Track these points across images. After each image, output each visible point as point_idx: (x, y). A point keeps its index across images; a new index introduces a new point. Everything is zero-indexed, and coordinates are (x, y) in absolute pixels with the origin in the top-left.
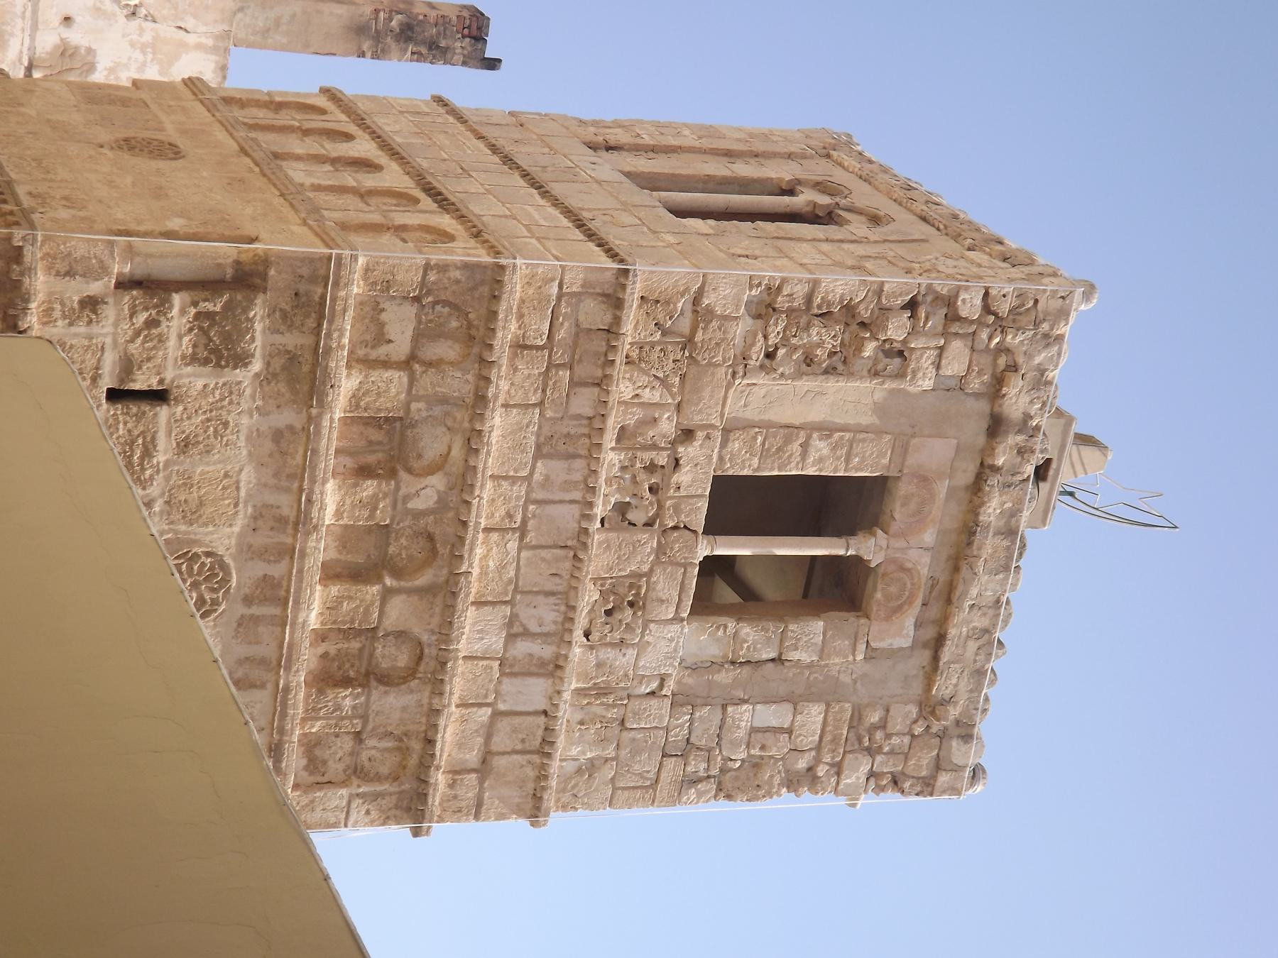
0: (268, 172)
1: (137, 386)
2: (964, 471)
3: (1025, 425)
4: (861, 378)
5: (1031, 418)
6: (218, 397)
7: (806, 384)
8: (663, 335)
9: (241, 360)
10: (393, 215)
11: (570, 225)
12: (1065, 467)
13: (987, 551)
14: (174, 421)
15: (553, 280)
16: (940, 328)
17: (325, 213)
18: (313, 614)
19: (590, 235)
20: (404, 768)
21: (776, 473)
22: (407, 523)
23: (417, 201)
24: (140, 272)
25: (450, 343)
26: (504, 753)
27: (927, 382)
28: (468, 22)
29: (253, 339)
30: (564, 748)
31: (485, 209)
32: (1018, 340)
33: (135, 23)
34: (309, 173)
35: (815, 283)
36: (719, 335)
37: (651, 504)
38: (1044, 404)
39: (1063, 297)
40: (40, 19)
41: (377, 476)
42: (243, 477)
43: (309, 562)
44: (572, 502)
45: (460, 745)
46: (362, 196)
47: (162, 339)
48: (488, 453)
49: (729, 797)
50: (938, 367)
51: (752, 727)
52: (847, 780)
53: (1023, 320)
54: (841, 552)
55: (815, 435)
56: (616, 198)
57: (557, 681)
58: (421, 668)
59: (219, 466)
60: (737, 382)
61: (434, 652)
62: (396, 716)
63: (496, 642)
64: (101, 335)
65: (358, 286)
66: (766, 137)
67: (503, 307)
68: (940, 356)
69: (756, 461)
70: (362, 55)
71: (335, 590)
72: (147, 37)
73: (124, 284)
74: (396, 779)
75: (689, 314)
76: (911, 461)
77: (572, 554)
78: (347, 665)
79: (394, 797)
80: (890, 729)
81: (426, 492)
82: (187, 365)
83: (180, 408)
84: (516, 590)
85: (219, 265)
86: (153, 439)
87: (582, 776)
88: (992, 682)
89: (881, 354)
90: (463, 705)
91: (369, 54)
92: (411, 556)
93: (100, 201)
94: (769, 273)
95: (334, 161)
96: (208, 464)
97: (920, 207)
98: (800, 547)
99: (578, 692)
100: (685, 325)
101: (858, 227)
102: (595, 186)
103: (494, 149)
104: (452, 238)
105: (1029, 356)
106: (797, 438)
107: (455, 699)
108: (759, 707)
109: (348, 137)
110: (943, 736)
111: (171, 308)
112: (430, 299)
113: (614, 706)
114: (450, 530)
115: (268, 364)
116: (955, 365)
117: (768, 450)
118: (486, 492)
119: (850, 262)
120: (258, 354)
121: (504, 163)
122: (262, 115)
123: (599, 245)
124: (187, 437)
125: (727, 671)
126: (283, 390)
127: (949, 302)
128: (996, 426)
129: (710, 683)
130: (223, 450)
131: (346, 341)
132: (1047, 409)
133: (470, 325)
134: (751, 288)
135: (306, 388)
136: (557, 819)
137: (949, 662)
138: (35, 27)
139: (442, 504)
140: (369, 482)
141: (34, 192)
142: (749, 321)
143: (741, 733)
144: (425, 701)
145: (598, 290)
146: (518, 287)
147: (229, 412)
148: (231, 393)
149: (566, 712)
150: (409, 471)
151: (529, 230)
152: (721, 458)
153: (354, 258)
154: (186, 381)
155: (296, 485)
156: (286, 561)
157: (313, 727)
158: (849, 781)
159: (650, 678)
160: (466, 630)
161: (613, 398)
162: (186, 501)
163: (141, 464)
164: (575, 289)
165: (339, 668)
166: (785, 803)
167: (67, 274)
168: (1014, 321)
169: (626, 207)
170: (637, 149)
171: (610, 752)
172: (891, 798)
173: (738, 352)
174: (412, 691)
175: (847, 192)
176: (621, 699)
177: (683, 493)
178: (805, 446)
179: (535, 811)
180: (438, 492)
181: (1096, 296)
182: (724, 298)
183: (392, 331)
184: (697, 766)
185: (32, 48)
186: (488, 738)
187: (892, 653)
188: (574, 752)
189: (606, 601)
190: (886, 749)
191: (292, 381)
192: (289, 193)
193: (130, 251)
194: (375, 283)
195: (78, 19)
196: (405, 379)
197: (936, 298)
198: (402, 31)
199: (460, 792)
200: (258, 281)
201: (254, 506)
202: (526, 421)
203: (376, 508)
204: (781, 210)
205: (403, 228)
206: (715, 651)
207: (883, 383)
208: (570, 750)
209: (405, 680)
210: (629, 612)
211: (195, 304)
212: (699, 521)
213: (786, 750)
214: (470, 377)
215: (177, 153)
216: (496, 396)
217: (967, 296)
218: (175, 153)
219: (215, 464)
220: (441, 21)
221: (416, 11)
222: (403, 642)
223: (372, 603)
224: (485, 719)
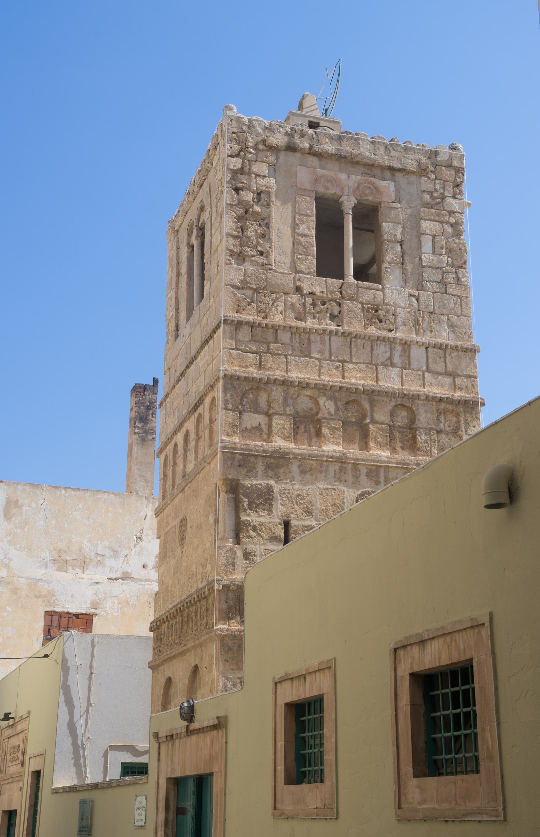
0: (190, 480)
2: (312, 161)
3: (290, 135)
4: (270, 211)
5: (287, 132)
6: (286, 499)
7: (274, 237)
8: (253, 302)
9: (270, 489)
10: (205, 425)
12: (312, 114)
13: (349, 149)
14: (297, 518)
15: (230, 353)
16: (247, 176)
17: (205, 454)
18: (383, 454)
19: (211, 337)
20: (453, 411)
21: (315, 248)
22: (341, 414)
23: (200, 414)
24: (232, 534)
25: (260, 397)
26: (446, 366)
27: (272, 181)
28: (138, 393)
29: (260, 484)
30: (443, 339)
32: (251, 140)
33: (143, 537)
34: (191, 462)
35: (228, 235)
36: (252, 277)
37: (330, 304)
38: (280, 126)
39: (231, 120)
40: (145, 578)
41: (320, 427)
42: (322, 487)
43: (360, 456)
44: (330, 340)
45: (442, 386)
46: (199, 438)
47: (261, 524)
48: (308, 378)
49: (465, 263)
50: (265, 176)
51: (432, 254)
52: (457, 208)
53: (242, 138)
54: (351, 216)
55: (297, 231)
56: (196, 325)
57: (412, 343)
58: (407, 405)
59: (317, 497)
60: (274, 268)
61: (399, 399)
62: (429, 415)
63: (394, 372)
64: (260, 550)
65: (235, 439)
66: (171, 259)
67: (243, 375)
68: (259, 176)
69: (310, 258)
71: (372, 445)
73: (238, 541)
74: (458, 414)
75: (244, 291)
76: (308, 187)
77: (353, 339)
78: (406, 438)
79: (467, 415)
81: (327, 406)
82: (272, 513)
83: (292, 515)
84: (371, 364)
85: (228, 500)
86: (306, 526)
87: (456, 330)
88: (410, 143)
89: (259, 203)
90: (424, 385)
91: (154, 436)
92: (356, 411)
94: (223, 255)
95: (186, 450)
96: (316, 502)
97: (196, 188)
98: (348, 235)
99: (417, 333)
100: (249, 293)
101: (205, 216)
102: (192, 335)
103: (178, 381)
104: (214, 398)
105: (258, 135)
106: (299, 239)
107: (421, 389)
108: (423, 251)
109: (176, 445)
110: (435, 165)
111: (247, 520)
112: (240, 407)
113: (423, 317)
114: (344, 394)
115: (271, 477)
117: (304, 252)
118: (326, 379)
119: (219, 219)
121: (184, 376)
122: (169, 483)
123: (215, 333)
124: (305, 512)
125: (406, 266)
126: (282, 470)
127: (235, 173)
128: (291, 148)
129: (412, 274)
130: (310, 496)
131: (260, 443)
132: (283, 125)
133: (251, 389)
134: (231, 264)
135: (281, 460)
136: (475, 342)
137: (401, 164)
138: (148, 580)
139: (332, 398)
140: (323, 431)
141: (201, 580)
142: (246, 264)
143: (435, 258)
144: (422, 402)
145: (234, 332)
146: (234, 368)
147: (293, 494)
148: (284, 493)
149: (427, 339)
150: (317, 413)
151: (210, 364)
152: (309, 273)
153: (222, 441)
154: (279, 513)
155: (325, 463)
156: (358, 466)
157: (435, 452)
158: (457, 208)
159: (410, 301)
160: (389, 385)
161: (282, 323)
162: (333, 512)
164: (234, 343)
165: (408, 441)
166: (468, 237)
168: (242, 143)
169: (200, 321)
170: (177, 317)
171: (444, 318)
172: (465, 187)
173: (260, 268)
174: (418, 409)
175: (191, 222)
176: (420, 314)
177: (325, 290)
178: (302, 235)
179: (472, 351)
180: (327, 400)
181: (230, 105)
182: (236, 275)
183: (255, 423)
184: (450, 279)
186: (439, 373)
187: (397, 191)
188: (445, 334)
189: (375, 323)
190: (442, 191)
191: (278, 467)
192: (198, 470)
193: (223, 539)
194: (234, 432)
195: (144, 562)
196: (276, 417)
197: (233, 179)
198: (143, 422)
199: (464, 385)
200: (234, 483)
201: (335, 481)
202: (294, 362)
203: (335, 428)
204: (200, 251)
206: (397, 272)
207: (273, 201)
208: (444, 336)
209: (413, 412)
211: (245, 510)
212: (337, 282)
213: (443, 237)
214: (274, 388)
216: (283, 376)
217: (232, 165)
218: (184, 520)
219: (316, 500)
220: (138, 405)
221: (134, 416)
222: (396, 413)
223: (378, 428)
224: (430, 375)
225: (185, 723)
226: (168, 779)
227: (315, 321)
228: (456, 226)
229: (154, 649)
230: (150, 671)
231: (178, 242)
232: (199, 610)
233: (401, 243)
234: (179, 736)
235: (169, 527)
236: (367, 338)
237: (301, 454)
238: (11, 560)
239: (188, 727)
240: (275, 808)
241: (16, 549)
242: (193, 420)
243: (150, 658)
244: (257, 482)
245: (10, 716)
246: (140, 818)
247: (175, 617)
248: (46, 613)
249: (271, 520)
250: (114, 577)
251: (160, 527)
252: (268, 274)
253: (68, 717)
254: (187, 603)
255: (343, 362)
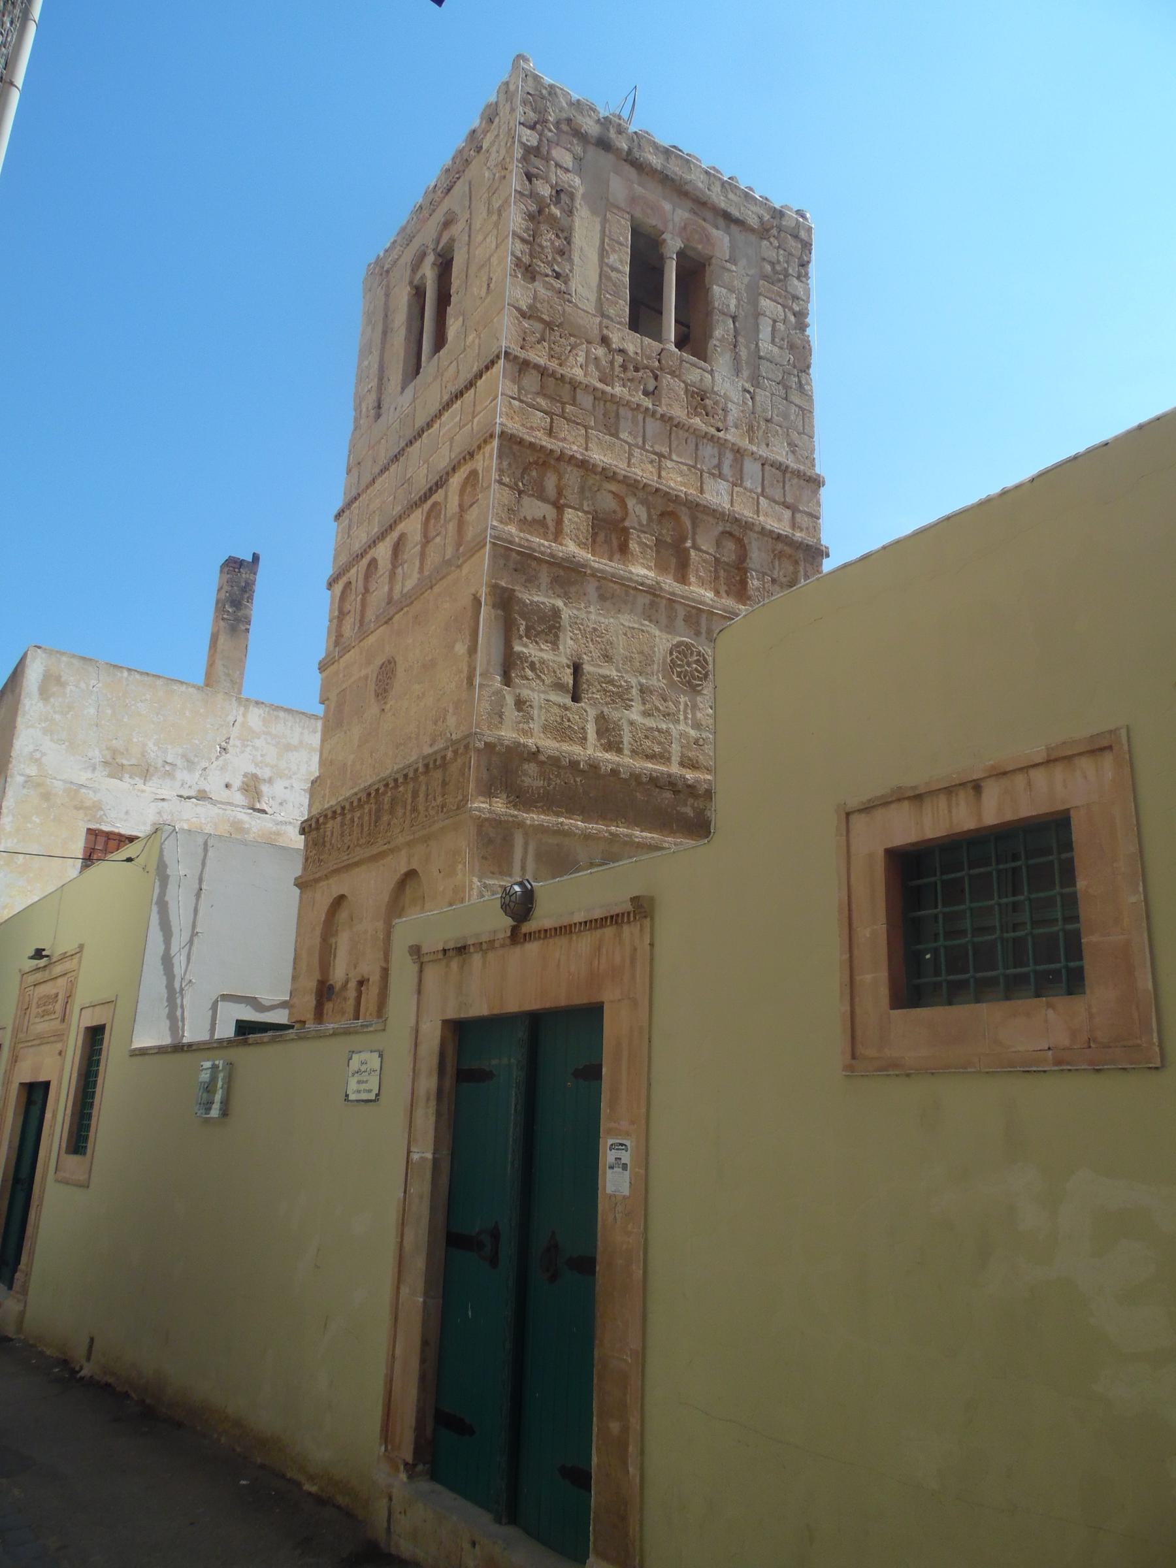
0: (408, 601)
1: (571, 682)
4: (573, 221)
7: (576, 259)
9: (556, 613)
11: (459, 402)
19: (471, 384)
20: (790, 556)
23: (435, 504)
24: (499, 669)
29: (543, 603)
31: (443, 459)
33: (230, 749)
35: (514, 233)
36: (545, 304)
42: (626, 624)
45: (780, 520)
46: (428, 542)
47: (542, 662)
49: (809, 367)
52: (801, 294)
58: (737, 534)
61: (728, 525)
63: (723, 486)
68: (561, 167)
70: (247, 630)
71: (693, 579)
72: (238, 743)
73: (507, 681)
74: (796, 562)
75: (531, 322)
76: (623, 205)
80: (774, 260)
81: (637, 511)
86: (603, 677)
88: (751, 189)
92: (675, 524)
93: (439, 700)
99: (751, 441)
100: (539, 326)
104: (474, 473)
105: (561, 109)
109: (373, 563)
110: (780, 229)
116: (567, 160)
119: (495, 218)
120: (552, 601)
121: (397, 460)
122: (349, 622)
123: (481, 377)
128: (604, 144)
131: (546, 543)
133: (536, 463)
136: (821, 468)
139: (643, 502)
142: (536, 283)
143: (776, 350)
144: (756, 535)
149: (763, 451)
150: (623, 520)
151: (464, 426)
152: (619, 323)
153: (494, 528)
159: (744, 398)
161: (585, 381)
163: (618, 687)
166: (814, 332)
167: (500, 717)
172: (813, 269)
177: (639, 351)
178: (613, 269)
183: (539, 515)
185: (243, 807)
187: (733, 247)
195: (227, 780)
199: (804, 526)
200: (506, 595)
205: (461, 506)
210: (707, 401)
211: (521, 637)
214: (569, 469)
215: (390, 662)
216: (582, 454)
225: (510, 922)
226: (445, 1022)
227: (625, 390)
228: (801, 315)
229: (307, 859)
230: (298, 891)
231: (388, 286)
232: (423, 787)
233: (734, 318)
234: (487, 947)
235: (352, 680)
236: (691, 430)
237: (602, 571)
238: (44, 754)
239: (514, 930)
240: (854, 1057)
241: (52, 740)
242: (418, 516)
243: (299, 873)
244: (540, 597)
245: (44, 953)
246: (363, 1087)
247: (360, 805)
248: (89, 830)
249: (556, 658)
250: (185, 795)
251: (325, 688)
252: (567, 308)
253: (163, 947)
254: (396, 780)
255: (661, 456)
